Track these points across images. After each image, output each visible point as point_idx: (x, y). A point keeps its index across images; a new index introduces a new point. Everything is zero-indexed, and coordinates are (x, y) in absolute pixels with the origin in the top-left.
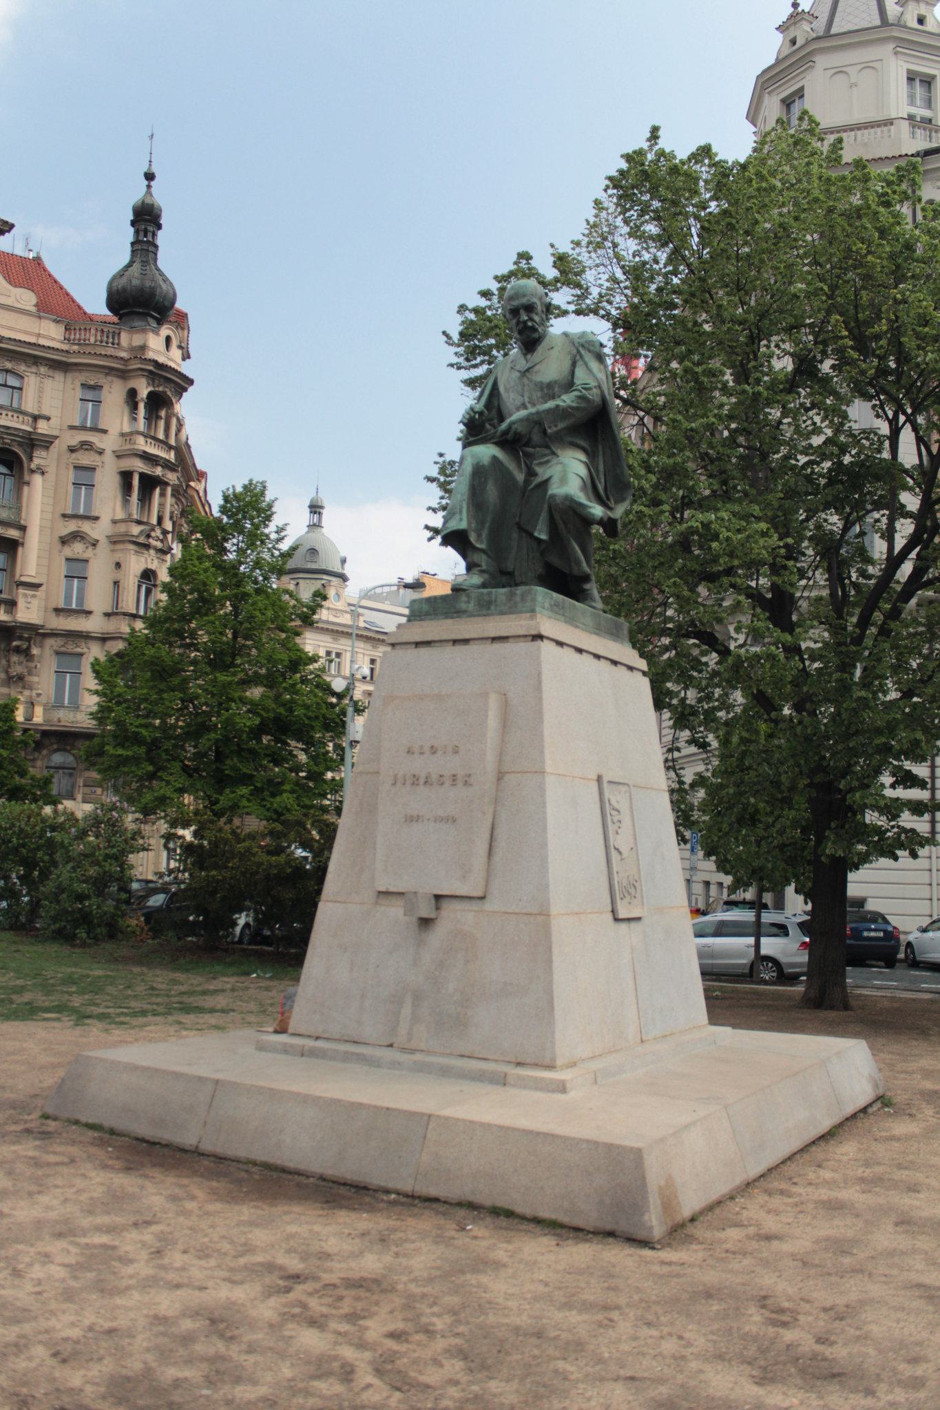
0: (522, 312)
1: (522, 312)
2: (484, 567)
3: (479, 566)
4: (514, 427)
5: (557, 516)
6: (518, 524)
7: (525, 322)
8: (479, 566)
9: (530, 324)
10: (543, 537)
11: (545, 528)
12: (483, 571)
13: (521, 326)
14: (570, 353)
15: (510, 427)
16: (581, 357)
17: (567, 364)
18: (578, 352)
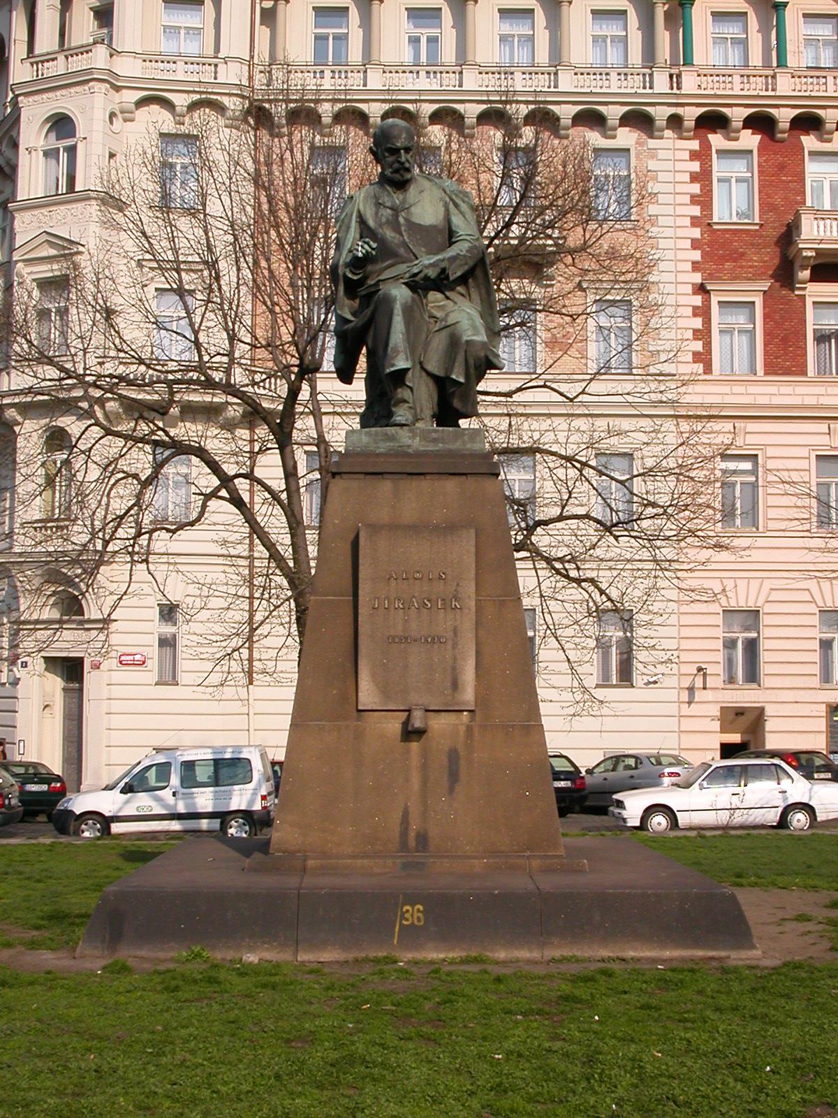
3: (405, 401)
4: (426, 271)
5: (471, 362)
6: (421, 363)
8: (405, 401)
9: (407, 165)
10: (462, 380)
11: (463, 373)
13: (396, 165)
14: (441, 199)
16: (456, 205)
17: (442, 210)
18: (452, 199)
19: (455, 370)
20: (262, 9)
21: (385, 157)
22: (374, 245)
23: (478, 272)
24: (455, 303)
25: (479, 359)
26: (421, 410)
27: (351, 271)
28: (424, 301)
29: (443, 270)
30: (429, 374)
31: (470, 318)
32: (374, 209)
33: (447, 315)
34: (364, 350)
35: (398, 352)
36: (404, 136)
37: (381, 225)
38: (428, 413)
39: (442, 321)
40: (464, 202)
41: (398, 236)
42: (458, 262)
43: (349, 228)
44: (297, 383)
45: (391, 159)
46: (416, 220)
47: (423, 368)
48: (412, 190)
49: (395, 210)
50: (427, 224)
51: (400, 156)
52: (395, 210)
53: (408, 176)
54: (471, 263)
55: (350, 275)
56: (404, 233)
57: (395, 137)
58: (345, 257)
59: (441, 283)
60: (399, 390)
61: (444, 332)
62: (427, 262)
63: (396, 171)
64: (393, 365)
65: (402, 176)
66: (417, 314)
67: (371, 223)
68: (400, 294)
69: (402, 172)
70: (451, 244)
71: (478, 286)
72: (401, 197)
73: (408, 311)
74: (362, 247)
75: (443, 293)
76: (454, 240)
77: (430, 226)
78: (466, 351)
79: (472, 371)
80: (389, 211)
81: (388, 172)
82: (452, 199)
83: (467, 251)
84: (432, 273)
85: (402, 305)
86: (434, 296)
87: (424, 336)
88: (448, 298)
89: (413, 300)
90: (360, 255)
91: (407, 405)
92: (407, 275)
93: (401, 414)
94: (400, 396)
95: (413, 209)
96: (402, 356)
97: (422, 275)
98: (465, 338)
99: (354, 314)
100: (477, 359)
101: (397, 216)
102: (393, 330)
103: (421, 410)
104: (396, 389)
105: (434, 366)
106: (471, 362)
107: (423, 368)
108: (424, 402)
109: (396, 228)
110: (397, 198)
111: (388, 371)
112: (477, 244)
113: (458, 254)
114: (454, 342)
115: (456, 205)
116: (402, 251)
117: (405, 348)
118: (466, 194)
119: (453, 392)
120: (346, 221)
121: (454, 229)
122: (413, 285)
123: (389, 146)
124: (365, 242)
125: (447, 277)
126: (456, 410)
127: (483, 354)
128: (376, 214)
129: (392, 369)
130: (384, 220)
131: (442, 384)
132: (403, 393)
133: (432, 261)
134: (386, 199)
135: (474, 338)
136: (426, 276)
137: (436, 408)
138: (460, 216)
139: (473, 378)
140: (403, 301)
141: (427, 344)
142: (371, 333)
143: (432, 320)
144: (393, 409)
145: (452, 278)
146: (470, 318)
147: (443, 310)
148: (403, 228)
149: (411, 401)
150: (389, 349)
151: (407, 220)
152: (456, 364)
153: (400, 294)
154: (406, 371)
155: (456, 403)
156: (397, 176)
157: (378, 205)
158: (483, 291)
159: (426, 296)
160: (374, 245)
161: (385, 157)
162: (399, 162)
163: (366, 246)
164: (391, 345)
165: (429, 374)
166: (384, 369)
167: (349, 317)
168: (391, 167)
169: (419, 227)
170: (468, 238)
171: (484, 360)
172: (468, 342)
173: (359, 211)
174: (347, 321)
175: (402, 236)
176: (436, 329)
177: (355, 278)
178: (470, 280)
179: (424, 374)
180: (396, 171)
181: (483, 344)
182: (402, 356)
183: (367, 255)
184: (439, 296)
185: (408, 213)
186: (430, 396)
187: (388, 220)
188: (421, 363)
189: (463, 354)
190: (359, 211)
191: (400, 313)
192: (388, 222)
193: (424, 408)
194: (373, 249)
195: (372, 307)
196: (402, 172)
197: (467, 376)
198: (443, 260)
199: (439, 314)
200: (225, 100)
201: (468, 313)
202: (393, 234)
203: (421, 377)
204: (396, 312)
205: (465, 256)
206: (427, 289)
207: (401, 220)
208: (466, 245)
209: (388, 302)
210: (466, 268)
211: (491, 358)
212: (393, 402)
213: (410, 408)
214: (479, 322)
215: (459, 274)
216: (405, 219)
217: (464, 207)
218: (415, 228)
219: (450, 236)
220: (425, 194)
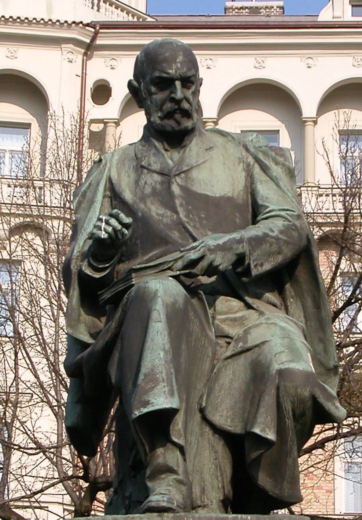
0: (178, 84)
1: (178, 84)
2: (180, 477)
3: (171, 470)
4: (210, 257)
5: (288, 406)
6: (202, 410)
7: (178, 102)
8: (171, 470)
9: (186, 105)
10: (271, 436)
11: (273, 424)
12: (180, 482)
13: (169, 106)
14: (241, 160)
15: (201, 258)
16: (264, 169)
18: (257, 160)
19: (260, 419)
20: (91, 132)
21: (151, 94)
22: (128, 220)
23: (301, 272)
24: (261, 313)
25: (302, 401)
26: (203, 491)
27: (90, 265)
28: (210, 312)
29: (240, 259)
30: (217, 430)
31: (286, 335)
32: (133, 176)
33: (246, 332)
34: (118, 398)
35: (156, 382)
36: (180, 58)
37: (143, 199)
38: (214, 496)
39: (238, 340)
40: (277, 163)
41: (169, 213)
42: (265, 247)
43: (92, 202)
44: (86, 503)
45: (159, 97)
46: (200, 188)
47: (205, 419)
48: (194, 147)
49: (166, 175)
50: (218, 196)
51: (174, 91)
52: (166, 175)
53: (188, 124)
54: (288, 252)
55: (88, 272)
56: (180, 209)
57: (165, 60)
58: (82, 243)
59: (238, 281)
60: (160, 451)
61: (242, 360)
62: (213, 244)
63: (169, 115)
64: (147, 403)
65: (178, 123)
66: (195, 327)
67: (128, 196)
68: (164, 289)
69: (178, 116)
70: (254, 222)
71: (300, 295)
72: (176, 155)
73: (178, 321)
74: (107, 223)
75: (241, 299)
76: (258, 218)
77: (221, 198)
78: (278, 389)
79: (289, 422)
80: (157, 178)
81: (156, 118)
82: (257, 160)
83: (281, 232)
84: (223, 261)
85: (166, 306)
86: (227, 305)
87: (207, 365)
88: (249, 306)
89: (187, 302)
90: (103, 235)
91: (175, 476)
92: (180, 264)
93: (162, 492)
94: (160, 460)
95: (194, 174)
96: (162, 387)
97: (204, 264)
98: (276, 366)
99: (93, 336)
100: (298, 402)
101: (169, 184)
102: (149, 344)
103: (203, 491)
104: (153, 448)
105: (225, 416)
106: (288, 406)
107: (205, 419)
108: (207, 477)
109: (166, 198)
110: (171, 158)
111: (137, 413)
112: (297, 223)
113: (266, 235)
114: (259, 374)
115: (264, 169)
116: (175, 235)
117: (168, 374)
118: (281, 152)
119: (259, 458)
120: (89, 194)
121: (260, 202)
122: (187, 276)
123: (157, 74)
124: (111, 215)
125: (248, 271)
126: (263, 492)
127: (306, 393)
128: (137, 182)
129: (145, 410)
130: (148, 190)
131: (239, 445)
132: (166, 456)
133: (221, 242)
134: (153, 159)
135: (292, 365)
136: (210, 265)
137: (228, 489)
138: (271, 184)
139: (291, 436)
140: (169, 300)
141: (212, 378)
142: (116, 356)
143: (222, 342)
144: (149, 484)
145: (254, 272)
146: (286, 335)
147: (242, 324)
148: (178, 202)
149: (181, 470)
150: (141, 377)
151: (184, 189)
152: (262, 410)
153: (164, 289)
154: (167, 415)
155: (264, 480)
156: (170, 124)
157: (141, 168)
158: (309, 302)
159: (212, 304)
160: (128, 220)
161: (151, 94)
162: (173, 100)
163: (113, 221)
164: (144, 370)
165: (217, 430)
166: (131, 413)
167: (87, 339)
168: (161, 110)
169: (206, 199)
170: (283, 213)
171: (309, 404)
172: (281, 372)
173: (110, 180)
174: (85, 345)
175: (177, 213)
176: (229, 354)
177: (97, 276)
178: (288, 286)
179: (207, 429)
180: (169, 115)
181: (308, 375)
182: (162, 387)
183: (115, 236)
184: (235, 303)
185: (187, 179)
186: (219, 467)
187: (154, 189)
188: (202, 410)
189: (274, 391)
190: (110, 180)
191: (163, 317)
192: (154, 193)
193: (208, 487)
194: (126, 226)
195: (120, 310)
196: (178, 116)
197: (281, 430)
198: (240, 241)
199: (233, 331)
200: (49, 224)
201: (283, 329)
202: (161, 211)
203: (202, 435)
204: (155, 315)
205: (277, 239)
206: (213, 293)
207: (175, 189)
208: (279, 223)
209: (145, 301)
210: (280, 259)
211: (321, 399)
212: (148, 472)
213: (180, 482)
214: (300, 341)
215: (267, 267)
216: (181, 187)
217: (277, 171)
218: (198, 202)
219: (256, 212)
220: (213, 153)
